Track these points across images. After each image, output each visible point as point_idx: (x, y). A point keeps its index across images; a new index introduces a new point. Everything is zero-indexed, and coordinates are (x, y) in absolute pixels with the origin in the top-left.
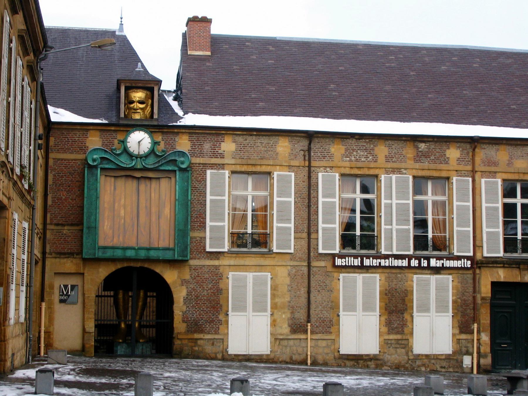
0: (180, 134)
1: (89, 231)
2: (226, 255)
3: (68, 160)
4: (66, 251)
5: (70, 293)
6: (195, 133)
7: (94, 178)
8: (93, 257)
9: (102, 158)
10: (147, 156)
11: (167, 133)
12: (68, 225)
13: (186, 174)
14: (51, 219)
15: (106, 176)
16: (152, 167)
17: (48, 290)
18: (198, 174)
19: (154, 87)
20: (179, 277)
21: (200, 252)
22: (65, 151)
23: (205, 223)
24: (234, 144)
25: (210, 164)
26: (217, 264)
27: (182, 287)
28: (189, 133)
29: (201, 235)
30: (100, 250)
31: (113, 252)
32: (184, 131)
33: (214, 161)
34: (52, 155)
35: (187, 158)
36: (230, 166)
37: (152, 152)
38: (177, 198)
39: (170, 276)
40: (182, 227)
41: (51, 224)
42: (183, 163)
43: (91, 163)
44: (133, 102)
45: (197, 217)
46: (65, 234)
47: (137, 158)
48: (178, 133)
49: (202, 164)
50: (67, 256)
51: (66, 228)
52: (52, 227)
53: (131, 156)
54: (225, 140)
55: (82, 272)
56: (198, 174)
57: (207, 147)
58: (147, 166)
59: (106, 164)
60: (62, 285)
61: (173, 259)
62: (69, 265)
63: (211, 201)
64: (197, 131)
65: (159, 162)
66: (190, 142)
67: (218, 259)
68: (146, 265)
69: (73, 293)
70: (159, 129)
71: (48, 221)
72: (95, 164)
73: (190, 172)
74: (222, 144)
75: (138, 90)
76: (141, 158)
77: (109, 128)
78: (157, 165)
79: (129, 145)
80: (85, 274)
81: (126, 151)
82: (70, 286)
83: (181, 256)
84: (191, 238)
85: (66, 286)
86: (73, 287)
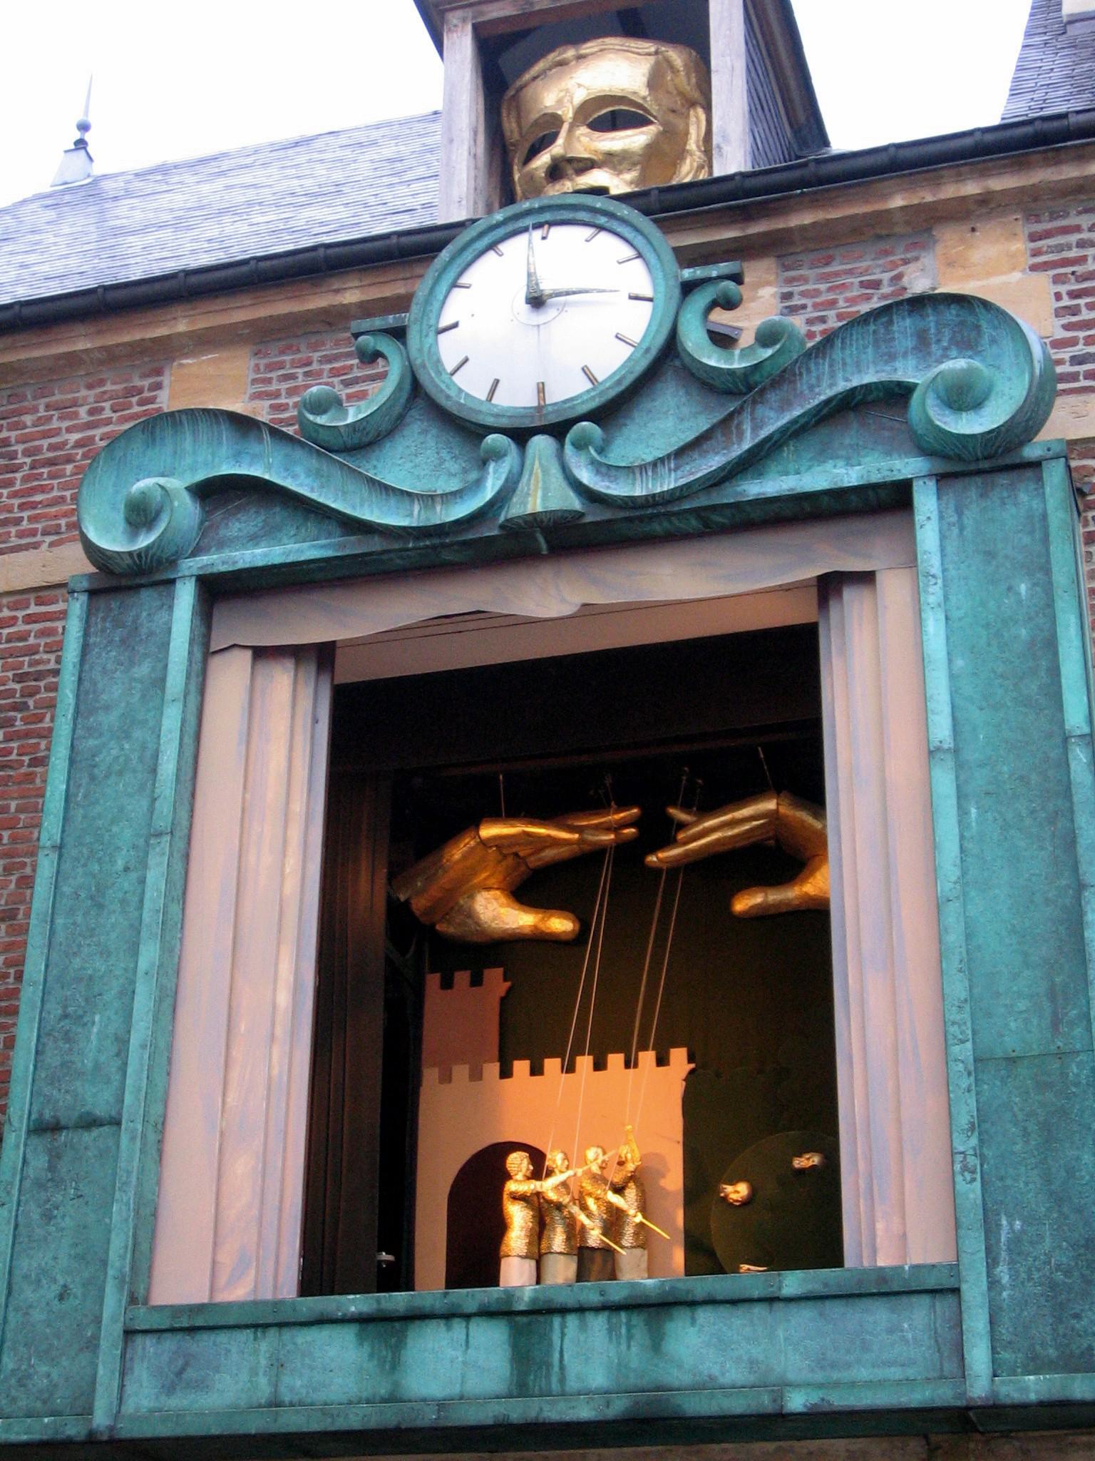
1: (55, 1156)
7: (143, 670)
9: (215, 493)
10: (613, 410)
11: (825, 242)
13: (1006, 510)
16: (667, 482)
28: (1030, 204)
30: (146, 1345)
31: (278, 1365)
32: (971, 188)
35: (1007, 345)
37: (665, 361)
38: (942, 730)
40: (1018, 1030)
42: (962, 396)
43: (113, 541)
44: (546, 132)
47: (520, 436)
48: (925, 224)
53: (467, 430)
59: (254, 539)
61: (942, 1395)
65: (726, 425)
66: (1044, 278)
70: (746, 215)
73: (1054, 475)
75: (589, 47)
76: (558, 430)
77: (318, 301)
78: (712, 462)
79: (449, 349)
81: (421, 400)
83: (1036, 1364)
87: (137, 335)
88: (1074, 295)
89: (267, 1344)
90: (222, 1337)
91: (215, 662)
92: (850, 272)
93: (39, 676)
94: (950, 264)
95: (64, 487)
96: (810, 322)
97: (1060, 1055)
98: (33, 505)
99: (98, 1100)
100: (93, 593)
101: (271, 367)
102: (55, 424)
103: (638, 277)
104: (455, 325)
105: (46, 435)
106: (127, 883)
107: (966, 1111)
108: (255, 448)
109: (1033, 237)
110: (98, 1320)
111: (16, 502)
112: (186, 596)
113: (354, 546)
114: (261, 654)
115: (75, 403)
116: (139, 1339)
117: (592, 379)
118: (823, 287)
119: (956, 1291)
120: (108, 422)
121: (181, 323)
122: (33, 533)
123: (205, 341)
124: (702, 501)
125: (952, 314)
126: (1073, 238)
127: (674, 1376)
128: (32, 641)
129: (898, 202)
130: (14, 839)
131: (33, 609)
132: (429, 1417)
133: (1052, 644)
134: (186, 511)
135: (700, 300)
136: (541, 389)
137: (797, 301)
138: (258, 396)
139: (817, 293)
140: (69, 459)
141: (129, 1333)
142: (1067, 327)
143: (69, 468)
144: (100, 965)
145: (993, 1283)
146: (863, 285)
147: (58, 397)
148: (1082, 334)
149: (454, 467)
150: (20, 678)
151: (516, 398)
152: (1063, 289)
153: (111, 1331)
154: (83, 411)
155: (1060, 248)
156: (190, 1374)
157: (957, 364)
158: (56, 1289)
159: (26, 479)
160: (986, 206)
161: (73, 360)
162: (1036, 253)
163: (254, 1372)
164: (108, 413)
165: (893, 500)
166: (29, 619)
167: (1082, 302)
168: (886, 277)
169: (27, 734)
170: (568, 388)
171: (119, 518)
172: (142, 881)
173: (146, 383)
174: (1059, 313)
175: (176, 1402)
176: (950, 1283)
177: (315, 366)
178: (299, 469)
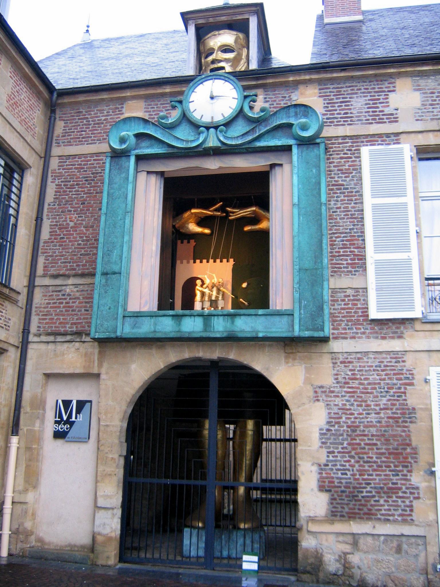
0: (301, 87)
1: (107, 280)
2: (418, 326)
3: (85, 155)
4: (68, 328)
5: (73, 419)
6: (332, 80)
7: (123, 175)
8: (113, 336)
9: (139, 136)
10: (228, 124)
11: (275, 86)
12: (75, 275)
13: (312, 153)
14: (45, 267)
15: (148, 173)
16: (240, 142)
17: (28, 409)
18: (341, 158)
19: (248, 20)
20: (307, 381)
21: (357, 323)
22: (80, 140)
23: (362, 258)
24: (418, 93)
25: (367, 136)
26: (397, 349)
27: (317, 403)
28: (320, 82)
29: (356, 282)
30: (128, 319)
31: (155, 324)
32: (307, 77)
33: (375, 129)
34: (56, 151)
35: (314, 116)
36: (413, 135)
37: (240, 114)
38: (296, 200)
39: (286, 377)
40: (308, 264)
41: (44, 276)
42: (304, 128)
43: (116, 146)
44: (211, 52)
45: (345, 247)
46: (69, 295)
47: (208, 128)
48: (296, 84)
49: (351, 137)
50: (68, 338)
51: (71, 281)
52: (47, 281)
53: (196, 126)
54: (397, 89)
55: (96, 371)
56: (341, 158)
57: (359, 105)
58: (229, 142)
59: (148, 147)
60: (60, 402)
61: (289, 335)
62: (72, 357)
63: (375, 207)
64: (335, 75)
66: (322, 99)
67: (400, 337)
68: (233, 355)
69: (81, 417)
70: (257, 79)
71: (40, 270)
72: (124, 146)
73: (322, 146)
74: (392, 95)
75: (221, 32)
76: (216, 128)
77: (160, 91)
78: (250, 138)
79: (192, 107)
80: (103, 376)
81: (185, 118)
82: (74, 403)
84: (334, 291)
85: (67, 403)
86: (81, 404)
87: (118, 95)
88: (328, 103)
89: (153, 320)
90: (144, 318)
91: (139, 174)
92: (279, 94)
93: (97, 173)
94: (301, 94)
95: (101, 130)
96: (270, 105)
97: (316, 269)
98: (94, 134)
99: (116, 268)
100: (112, 157)
101: (149, 105)
102: (99, 115)
103: (234, 93)
104: (193, 101)
105: (97, 117)
106: (121, 222)
107: (296, 280)
108: (148, 126)
109: (320, 89)
110: (117, 314)
111: (90, 132)
112: (133, 159)
113: (170, 151)
114: (148, 173)
115: (103, 110)
116: (126, 318)
117: (224, 116)
118: (273, 97)
119: (293, 315)
120: (111, 115)
121: (128, 93)
122: (94, 140)
123: (133, 98)
124: (247, 146)
125: (303, 108)
126: (329, 90)
127: (236, 329)
128: (95, 165)
129: (291, 79)
130: (93, 210)
131: (95, 158)
132: (187, 335)
133: (319, 183)
134: (133, 140)
135: (248, 100)
136: (212, 118)
137: (267, 100)
138: (146, 112)
139: (272, 98)
140: (102, 123)
141: (124, 317)
142: (326, 111)
143: (102, 125)
144: (115, 240)
145: (300, 314)
146: (283, 97)
147: (99, 108)
148: (329, 113)
149: (192, 134)
150: (93, 174)
151: (207, 119)
152: (326, 102)
153: (120, 316)
154: (105, 112)
155: (325, 92)
156: (137, 325)
157: (303, 120)
158: (108, 307)
159: (92, 127)
160: (310, 81)
161: (103, 100)
162: (320, 93)
163: (150, 325)
164: (111, 113)
165: (288, 149)
166: (94, 160)
167: (329, 105)
168: (287, 96)
169: (95, 187)
170: (218, 118)
171: (118, 141)
172: (124, 222)
173: (120, 106)
174: (325, 107)
175: (135, 331)
176: (292, 313)
177: (159, 106)
178: (158, 132)
